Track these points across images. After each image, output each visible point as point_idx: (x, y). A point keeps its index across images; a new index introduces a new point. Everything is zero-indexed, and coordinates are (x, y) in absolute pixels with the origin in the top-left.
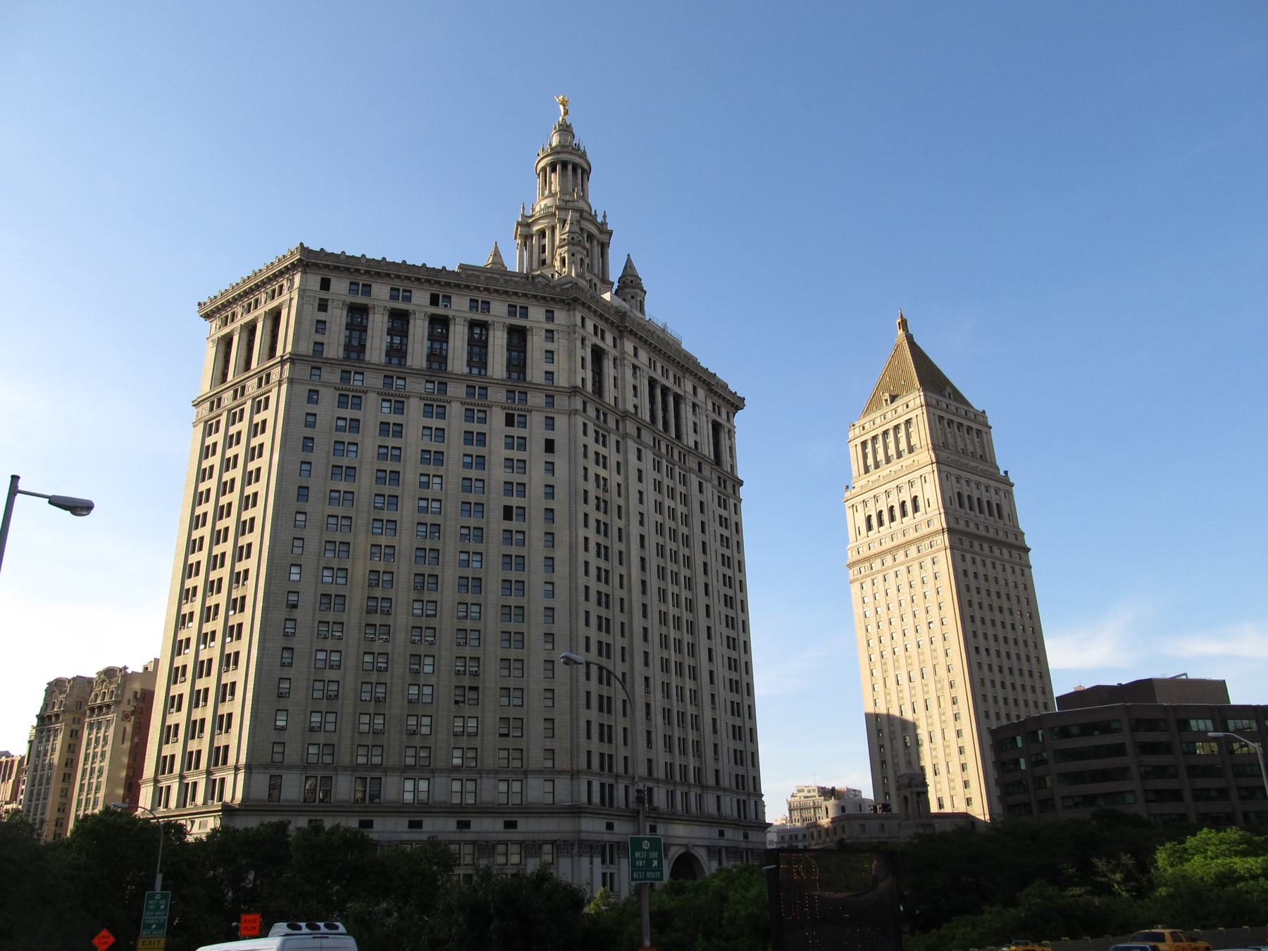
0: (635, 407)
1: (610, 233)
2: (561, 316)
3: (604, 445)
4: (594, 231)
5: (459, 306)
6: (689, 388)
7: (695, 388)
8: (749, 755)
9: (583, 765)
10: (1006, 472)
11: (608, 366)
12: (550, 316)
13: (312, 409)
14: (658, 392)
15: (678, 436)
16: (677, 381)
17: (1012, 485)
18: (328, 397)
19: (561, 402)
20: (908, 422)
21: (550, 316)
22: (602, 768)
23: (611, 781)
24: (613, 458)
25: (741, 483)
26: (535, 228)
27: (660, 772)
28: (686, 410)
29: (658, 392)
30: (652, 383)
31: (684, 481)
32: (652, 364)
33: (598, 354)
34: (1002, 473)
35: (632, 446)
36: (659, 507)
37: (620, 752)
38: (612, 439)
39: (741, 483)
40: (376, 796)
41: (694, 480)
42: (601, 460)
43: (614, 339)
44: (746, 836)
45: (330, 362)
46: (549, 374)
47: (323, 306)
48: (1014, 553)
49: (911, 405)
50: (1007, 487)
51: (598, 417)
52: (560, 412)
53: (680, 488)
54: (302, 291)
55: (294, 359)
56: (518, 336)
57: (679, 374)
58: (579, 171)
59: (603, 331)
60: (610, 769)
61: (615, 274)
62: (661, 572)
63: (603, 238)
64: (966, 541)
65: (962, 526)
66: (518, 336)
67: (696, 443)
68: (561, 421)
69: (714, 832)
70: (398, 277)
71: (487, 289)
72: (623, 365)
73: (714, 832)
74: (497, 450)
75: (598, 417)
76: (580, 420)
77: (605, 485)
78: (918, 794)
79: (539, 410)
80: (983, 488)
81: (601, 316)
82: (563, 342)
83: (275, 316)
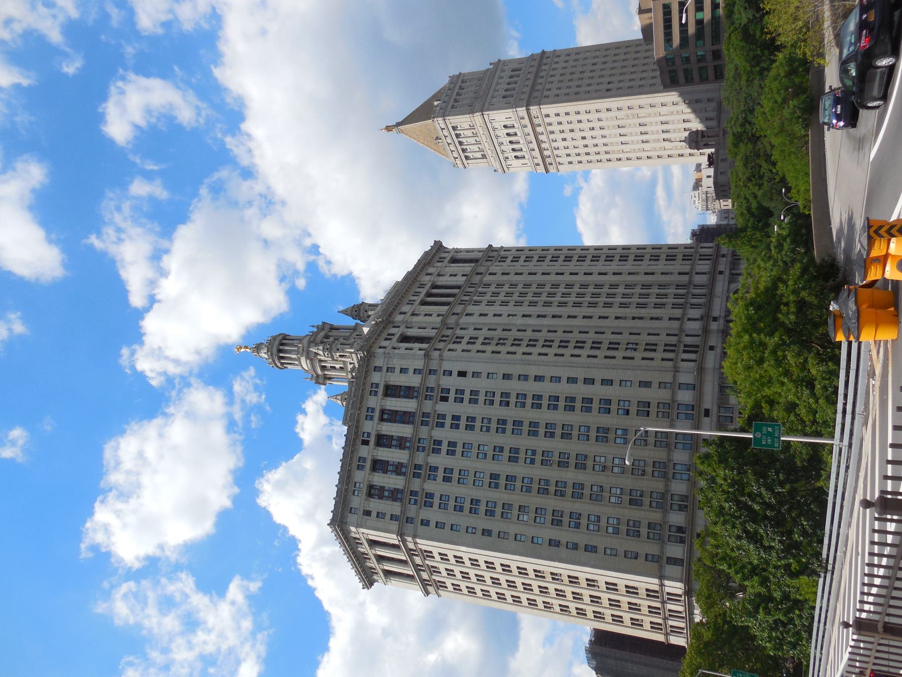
0: (439, 315)
1: (324, 323)
2: (379, 362)
3: (463, 338)
4: (322, 334)
5: (370, 427)
6: (428, 278)
7: (427, 274)
8: (670, 251)
9: (670, 364)
10: (491, 64)
12: (378, 369)
14: (429, 299)
15: (459, 287)
16: (422, 286)
17: (499, 60)
18: (425, 514)
19: (434, 365)
20: (454, 128)
21: (378, 369)
22: (673, 351)
23: (682, 346)
24: (471, 332)
25: (490, 246)
26: (319, 372)
27: (678, 313)
28: (442, 281)
29: (429, 299)
30: (424, 303)
31: (488, 285)
32: (411, 303)
33: (405, 339)
34: (491, 67)
35: (464, 320)
36: (504, 303)
37: (663, 339)
38: (459, 332)
39: (490, 246)
40: (680, 529)
41: (488, 278)
42: (472, 341)
43: (394, 327)
44: (724, 256)
45: (403, 512)
47: (368, 513)
48: (545, 61)
49: (443, 126)
50: (501, 64)
51: (445, 341)
52: (440, 366)
53: (493, 288)
54: (358, 526)
55: (401, 534)
56: (391, 391)
57: (418, 284)
58: (284, 341)
59: (389, 335)
60: (675, 346)
61: (351, 322)
62: (547, 304)
63: (327, 328)
64: (536, 94)
65: (525, 96)
66: (391, 391)
67: (463, 275)
68: (446, 366)
69: (720, 277)
70: (350, 464)
71: (360, 409)
72: (411, 323)
73: (720, 277)
74: (465, 409)
75: (445, 341)
76: (446, 354)
77: (488, 339)
78: (703, 136)
79: (438, 380)
80: (500, 81)
81: (379, 335)
82: (395, 361)
83: (373, 543)
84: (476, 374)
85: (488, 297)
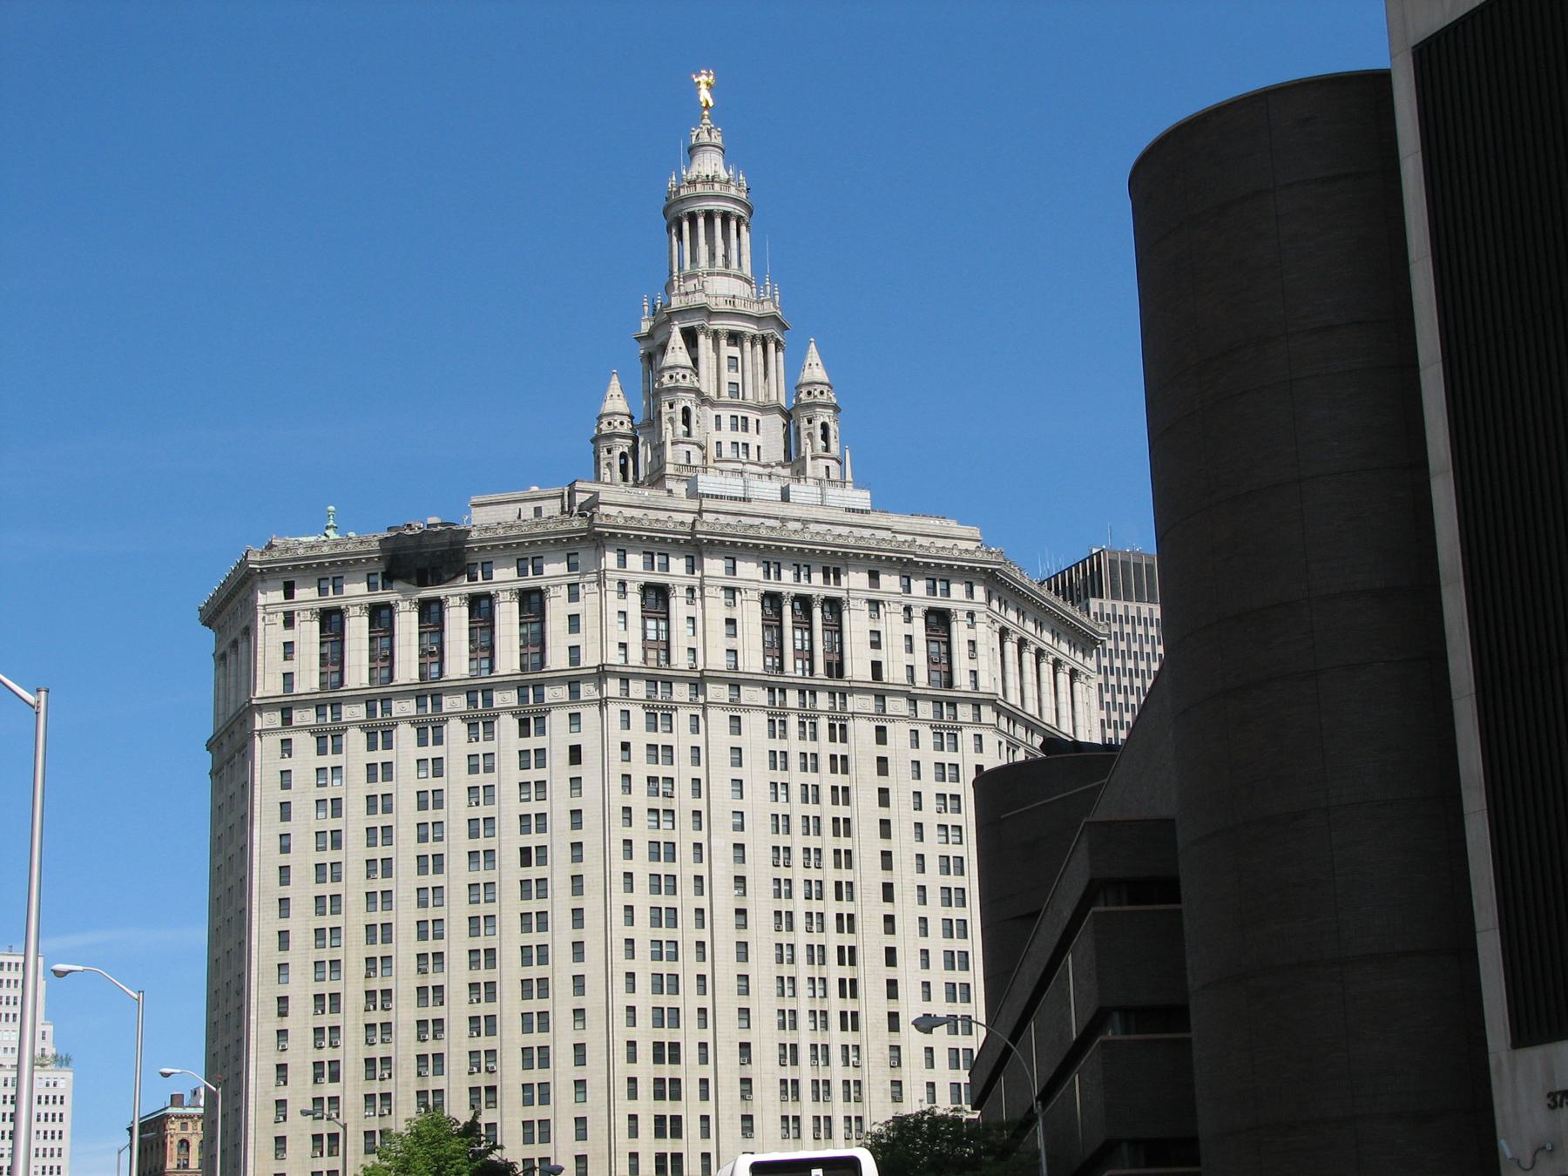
11: (679, 607)
13: (286, 764)
18: (304, 743)
19: (587, 691)
30: (772, 601)
33: (657, 597)
35: (718, 719)
41: (862, 731)
46: (574, 650)
53: (825, 747)
66: (532, 603)
67: (876, 666)
68: (589, 715)
74: (509, 775)
79: (561, 705)
84: (576, 782)
85: (794, 745)
